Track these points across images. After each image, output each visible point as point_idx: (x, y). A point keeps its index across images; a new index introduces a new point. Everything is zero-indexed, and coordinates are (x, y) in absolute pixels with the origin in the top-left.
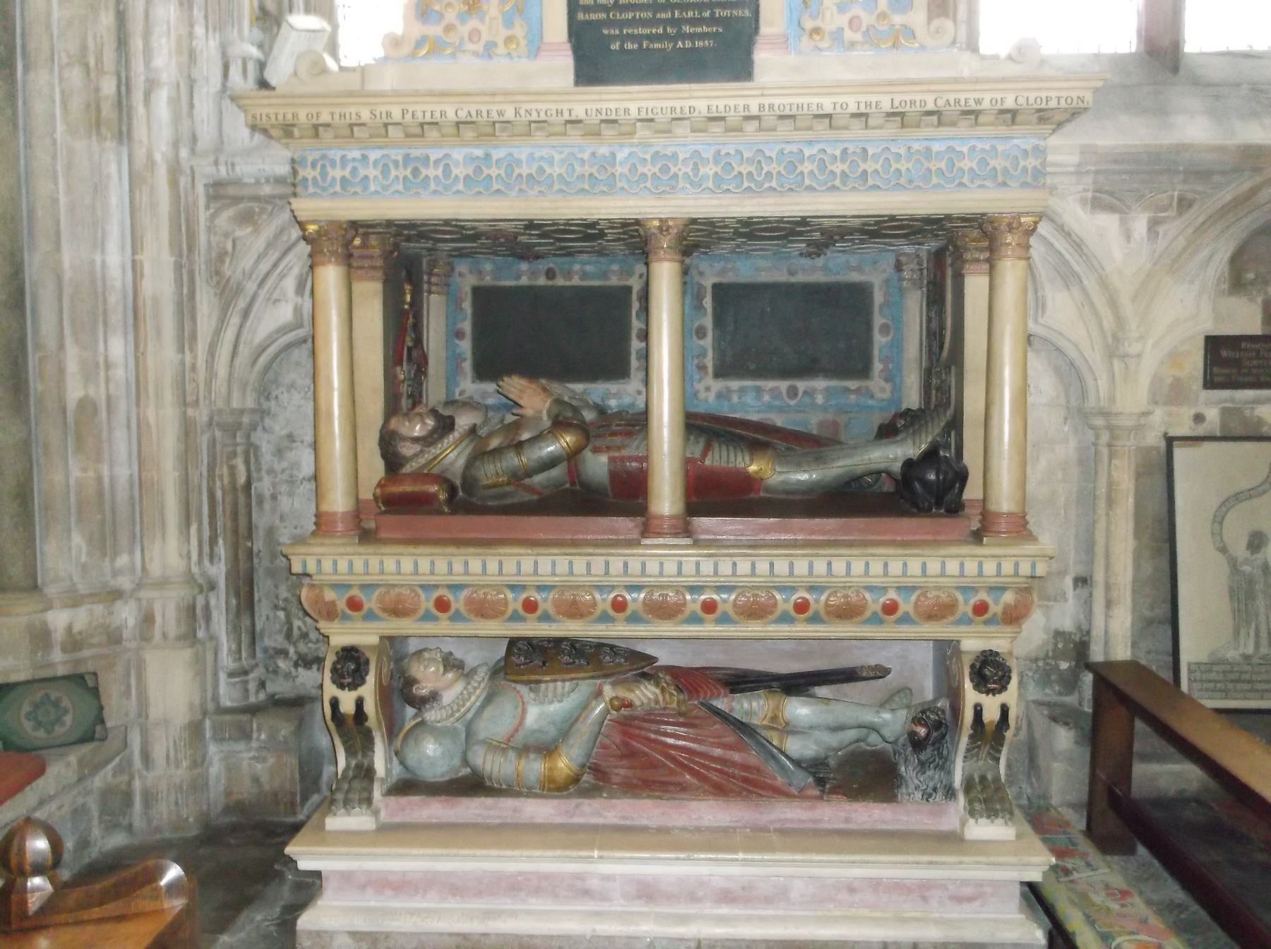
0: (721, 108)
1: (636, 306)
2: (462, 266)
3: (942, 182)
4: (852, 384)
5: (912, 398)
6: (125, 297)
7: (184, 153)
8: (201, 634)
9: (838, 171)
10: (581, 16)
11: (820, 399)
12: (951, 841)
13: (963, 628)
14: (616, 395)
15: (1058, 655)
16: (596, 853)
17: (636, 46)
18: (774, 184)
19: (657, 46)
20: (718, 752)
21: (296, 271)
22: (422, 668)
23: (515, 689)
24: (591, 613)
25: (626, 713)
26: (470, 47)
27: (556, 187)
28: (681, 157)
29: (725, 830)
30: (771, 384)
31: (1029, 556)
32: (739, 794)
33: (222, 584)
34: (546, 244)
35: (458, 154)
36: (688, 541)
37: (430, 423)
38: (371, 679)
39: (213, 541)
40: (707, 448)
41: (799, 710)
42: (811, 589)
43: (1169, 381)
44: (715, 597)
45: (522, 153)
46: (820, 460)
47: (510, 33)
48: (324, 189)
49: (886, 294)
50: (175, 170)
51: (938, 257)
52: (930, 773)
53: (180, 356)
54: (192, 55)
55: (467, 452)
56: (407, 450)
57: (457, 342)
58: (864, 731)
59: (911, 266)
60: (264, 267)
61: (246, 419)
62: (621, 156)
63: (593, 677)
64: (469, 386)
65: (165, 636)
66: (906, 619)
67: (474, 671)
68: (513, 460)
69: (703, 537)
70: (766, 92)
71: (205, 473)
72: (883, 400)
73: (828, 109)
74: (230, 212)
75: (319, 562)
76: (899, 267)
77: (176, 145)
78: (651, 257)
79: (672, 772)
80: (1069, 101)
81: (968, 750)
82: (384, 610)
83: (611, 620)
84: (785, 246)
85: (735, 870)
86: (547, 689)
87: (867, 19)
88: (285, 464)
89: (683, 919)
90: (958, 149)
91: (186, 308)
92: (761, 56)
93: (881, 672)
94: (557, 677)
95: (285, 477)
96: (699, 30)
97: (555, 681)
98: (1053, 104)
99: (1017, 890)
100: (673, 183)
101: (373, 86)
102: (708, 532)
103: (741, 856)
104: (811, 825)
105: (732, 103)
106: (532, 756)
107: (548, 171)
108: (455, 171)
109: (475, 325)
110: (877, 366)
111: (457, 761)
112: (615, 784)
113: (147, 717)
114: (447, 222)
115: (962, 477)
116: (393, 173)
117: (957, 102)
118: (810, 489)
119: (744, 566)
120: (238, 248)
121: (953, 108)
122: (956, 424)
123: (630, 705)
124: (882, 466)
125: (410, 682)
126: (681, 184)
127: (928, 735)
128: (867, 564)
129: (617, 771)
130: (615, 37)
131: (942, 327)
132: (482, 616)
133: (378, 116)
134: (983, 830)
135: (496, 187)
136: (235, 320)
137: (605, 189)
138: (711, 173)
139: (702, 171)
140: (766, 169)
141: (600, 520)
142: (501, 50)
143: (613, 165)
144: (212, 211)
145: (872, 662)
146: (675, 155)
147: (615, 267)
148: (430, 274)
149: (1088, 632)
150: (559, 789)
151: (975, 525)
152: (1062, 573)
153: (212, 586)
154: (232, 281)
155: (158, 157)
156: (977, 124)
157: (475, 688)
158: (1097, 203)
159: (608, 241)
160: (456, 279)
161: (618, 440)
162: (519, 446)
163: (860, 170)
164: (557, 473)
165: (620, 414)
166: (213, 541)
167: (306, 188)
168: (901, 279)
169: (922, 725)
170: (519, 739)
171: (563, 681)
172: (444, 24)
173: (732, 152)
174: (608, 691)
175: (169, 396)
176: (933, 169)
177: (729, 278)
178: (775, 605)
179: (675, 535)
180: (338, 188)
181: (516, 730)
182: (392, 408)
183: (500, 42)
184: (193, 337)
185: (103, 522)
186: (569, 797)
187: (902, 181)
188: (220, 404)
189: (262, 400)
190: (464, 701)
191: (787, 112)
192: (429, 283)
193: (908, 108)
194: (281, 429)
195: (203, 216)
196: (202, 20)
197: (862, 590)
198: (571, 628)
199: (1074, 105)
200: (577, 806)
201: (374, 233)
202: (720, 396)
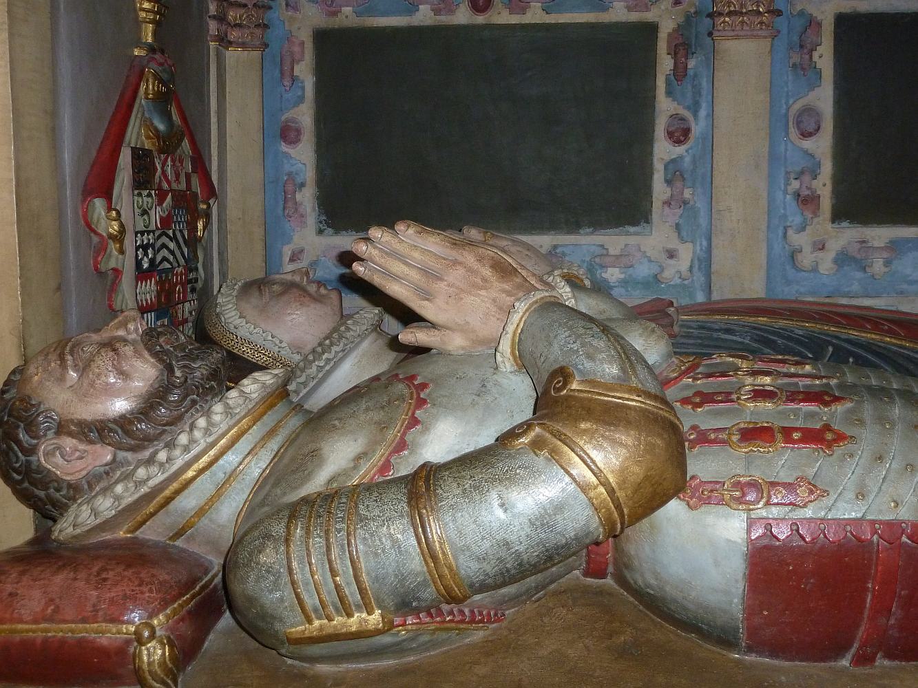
14: (622, 259)
57: (284, 147)
109: (321, 118)
202: (843, 259)
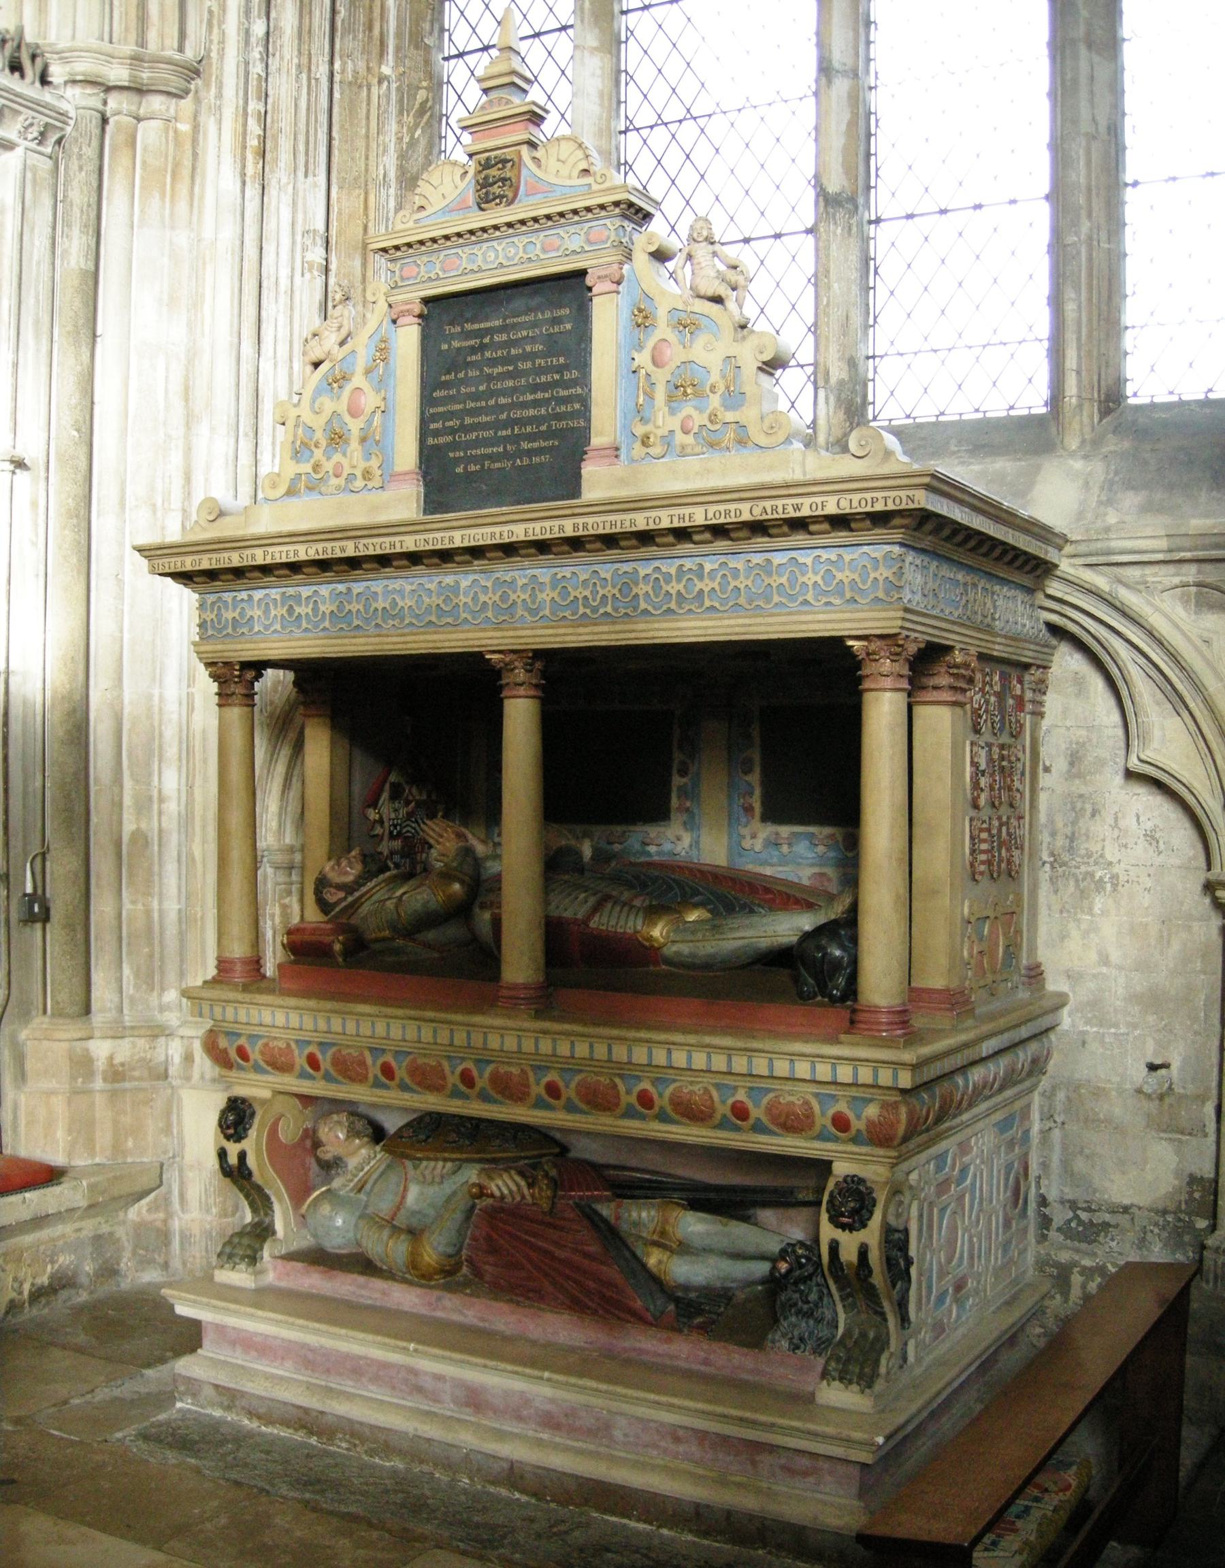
1: (677, 733)
3: (784, 600)
6: (181, 731)
9: (673, 592)
10: (430, 441)
17: (478, 467)
18: (609, 609)
19: (497, 465)
26: (334, 481)
27: (407, 622)
28: (520, 582)
30: (827, 830)
32: (595, 1312)
35: (324, 590)
40: (596, 909)
47: (368, 464)
65: (202, 1077)
66: (758, 1128)
80: (898, 501)
82: (268, 1063)
87: (700, 419)
89: (501, 1435)
90: (801, 560)
92: (589, 470)
96: (536, 445)
97: (436, 1159)
105: (547, 524)
107: (401, 604)
108: (322, 608)
116: (273, 613)
121: (770, 517)
125: (317, 1144)
127: (789, 1271)
130: (457, 461)
135: (356, 622)
138: (548, 599)
139: (541, 596)
140: (601, 592)
142: (359, 483)
143: (457, 596)
146: (514, 581)
163: (697, 589)
170: (401, 1221)
171: (445, 1160)
172: (312, 461)
173: (569, 575)
176: (774, 585)
178: (618, 1096)
180: (230, 630)
185: (151, 956)
186: (431, 1287)
187: (742, 601)
199: (903, 506)
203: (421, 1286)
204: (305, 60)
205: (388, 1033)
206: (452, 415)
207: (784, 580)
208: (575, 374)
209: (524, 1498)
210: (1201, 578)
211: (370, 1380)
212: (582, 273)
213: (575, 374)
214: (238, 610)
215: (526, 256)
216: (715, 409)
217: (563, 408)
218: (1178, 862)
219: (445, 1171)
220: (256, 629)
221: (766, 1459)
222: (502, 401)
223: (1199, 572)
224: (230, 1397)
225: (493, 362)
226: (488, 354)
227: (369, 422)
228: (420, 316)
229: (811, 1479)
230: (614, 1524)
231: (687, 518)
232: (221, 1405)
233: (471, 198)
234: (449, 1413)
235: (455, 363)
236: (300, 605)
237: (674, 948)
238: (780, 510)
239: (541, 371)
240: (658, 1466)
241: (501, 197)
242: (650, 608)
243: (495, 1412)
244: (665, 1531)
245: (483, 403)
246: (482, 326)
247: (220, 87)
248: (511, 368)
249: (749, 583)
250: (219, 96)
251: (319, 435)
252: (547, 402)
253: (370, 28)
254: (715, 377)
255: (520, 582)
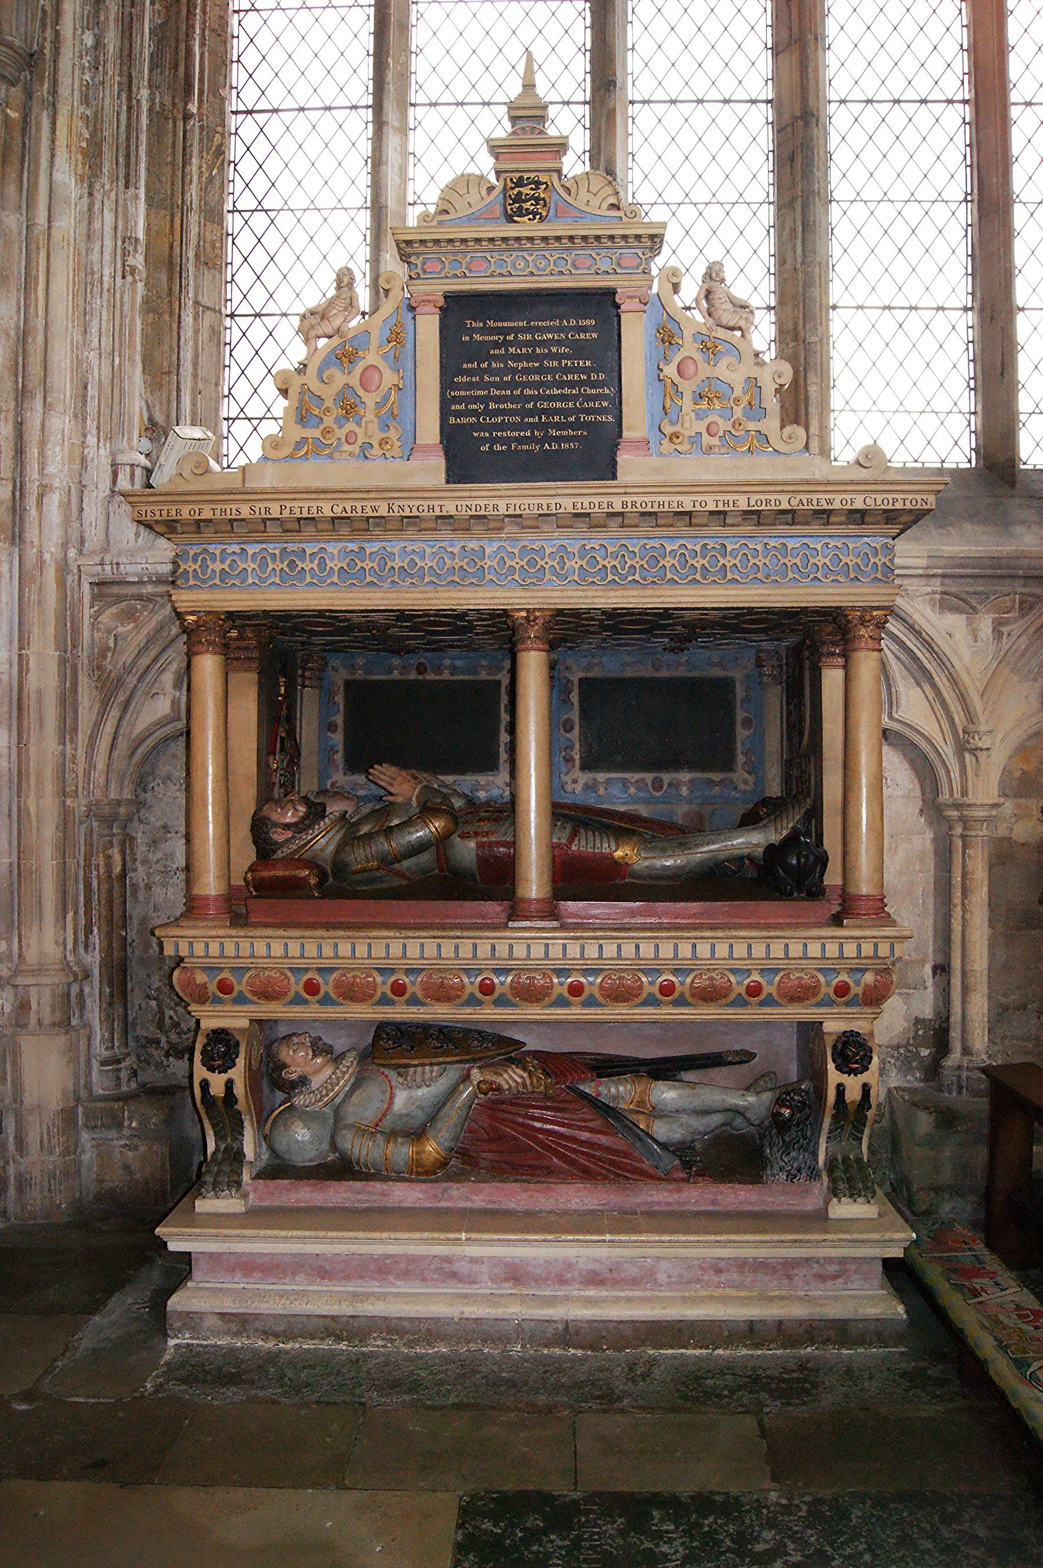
0: (586, 505)
1: (505, 699)
2: (335, 661)
4: (717, 777)
5: (774, 789)
7: (72, 553)
8: (74, 1022)
10: (452, 420)
11: (684, 791)
12: (820, 1219)
13: (824, 1010)
15: (918, 1041)
16: (464, 1236)
17: (504, 448)
18: (637, 577)
20: (585, 1135)
21: (174, 666)
22: (291, 1053)
23: (383, 1073)
24: (459, 996)
25: (493, 1097)
26: (346, 447)
27: (427, 580)
28: (548, 551)
29: (591, 1212)
30: (637, 776)
31: (888, 938)
32: (606, 1178)
33: (96, 972)
34: (417, 637)
35: (333, 548)
36: (555, 924)
37: (302, 809)
38: (240, 1062)
39: (88, 931)
40: (575, 833)
41: (666, 1094)
42: (676, 972)
43: (1018, 774)
44: (582, 980)
45: (395, 547)
46: (684, 846)
47: (384, 435)
48: (204, 581)
49: (748, 689)
50: (63, 569)
51: (796, 652)
52: (793, 1154)
53: (61, 747)
54: (84, 462)
55: (338, 838)
56: (279, 836)
57: (329, 734)
58: (730, 1114)
59: (772, 663)
60: (145, 662)
61: (122, 810)
62: (488, 550)
63: (460, 1062)
64: (340, 777)
65: (40, 1022)
66: (770, 1001)
67: (342, 1056)
68: (382, 845)
69: (570, 921)
70: (628, 490)
71: (82, 863)
72: (745, 792)
73: (688, 508)
74: (114, 610)
75: (191, 944)
76: (759, 665)
77: (65, 546)
78: (520, 647)
79: (541, 1157)
80: (914, 503)
81: (831, 1131)
83: (480, 1003)
84: (648, 641)
85: (603, 1252)
86: (415, 1073)
87: (724, 426)
88: (159, 855)
89: (550, 1301)
91: (68, 700)
93: (746, 1057)
94: (427, 1061)
95: (159, 867)
96: (565, 433)
97: (423, 1065)
98: (899, 506)
99: (879, 1267)
100: (540, 575)
101: (252, 484)
102: (574, 915)
103: (608, 1237)
104: (677, 1208)
105: (596, 500)
106: (400, 1140)
107: (420, 564)
108: (330, 564)
110: (741, 759)
111: (325, 1146)
112: (483, 1168)
113: (22, 1102)
114: (321, 613)
115: (823, 861)
116: (271, 566)
117: (810, 502)
118: (675, 874)
119: (610, 950)
120: (120, 643)
122: (815, 813)
123: (499, 1089)
124: (746, 851)
126: (548, 576)
127: (792, 1115)
128: (731, 946)
129: (484, 1155)
130: (485, 441)
131: (801, 719)
132: (352, 999)
133: (258, 513)
134: (844, 1209)
135: (369, 579)
136: (115, 713)
137: (474, 581)
138: (577, 566)
140: (629, 563)
141: (467, 903)
142: (376, 451)
144: (96, 608)
145: (738, 1047)
147: (484, 663)
148: (304, 669)
149: (948, 1019)
150: (427, 1173)
151: (836, 909)
152: (922, 962)
153: (87, 976)
154: (113, 675)
155: (47, 557)
156: (828, 523)
157: (344, 1073)
158: (947, 602)
159: (477, 634)
160: (329, 672)
161: (486, 826)
162: (388, 832)
163: (720, 565)
164: (425, 858)
165: (487, 803)
166: (88, 931)
167: (187, 580)
168: (761, 675)
169: (788, 1107)
170: (387, 1123)
171: (431, 1064)
172: (322, 427)
174: (476, 1075)
175: (49, 788)
176: (789, 564)
177: (596, 673)
178: (641, 987)
179: (542, 918)
180: (217, 581)
181: (385, 1115)
182: (265, 797)
183: (376, 444)
184: (75, 729)
186: (436, 1181)
187: (759, 576)
188: (98, 794)
189: (139, 791)
190: (334, 1085)
191: (649, 509)
192: (303, 676)
193: (763, 507)
194: (157, 820)
195: (87, 612)
196: (94, 431)
197: (726, 972)
198: (439, 1011)
199: (919, 507)
200: (445, 1190)
201: (249, 625)
202: (586, 787)
203: (424, 1181)
204: (125, 79)
205: (405, 953)
206: (476, 399)
207: (797, 561)
208: (602, 376)
209: (579, 1353)
210: (946, 589)
211: (398, 1277)
212: (611, 293)
213: (602, 376)
214: (228, 562)
215: (557, 270)
216: (738, 418)
217: (591, 404)
218: (901, 793)
219: (434, 1074)
220: (250, 581)
221: (800, 1272)
222: (528, 392)
223: (942, 584)
224: (241, 1322)
225: (517, 358)
226: (512, 350)
227: (386, 398)
228: (441, 308)
229: (841, 1281)
230: (674, 1357)
231: (731, 504)
232: (228, 1332)
233: (498, 210)
234: (489, 1291)
235: (479, 352)
236: (303, 560)
237: (647, 863)
238: (815, 503)
239: (567, 370)
240: (706, 1297)
241: (535, 214)
242: (676, 578)
243: (536, 1281)
244: (720, 1352)
245: (509, 392)
246: (505, 324)
247: (55, 83)
248: (536, 365)
249: (766, 561)
250: (54, 92)
251: (329, 403)
252: (574, 398)
253: (176, 66)
254: (738, 392)
255: (548, 551)
